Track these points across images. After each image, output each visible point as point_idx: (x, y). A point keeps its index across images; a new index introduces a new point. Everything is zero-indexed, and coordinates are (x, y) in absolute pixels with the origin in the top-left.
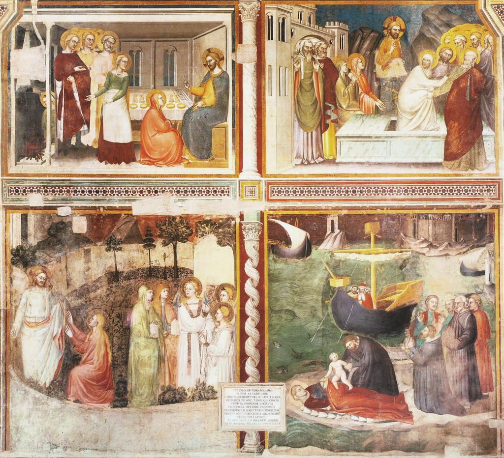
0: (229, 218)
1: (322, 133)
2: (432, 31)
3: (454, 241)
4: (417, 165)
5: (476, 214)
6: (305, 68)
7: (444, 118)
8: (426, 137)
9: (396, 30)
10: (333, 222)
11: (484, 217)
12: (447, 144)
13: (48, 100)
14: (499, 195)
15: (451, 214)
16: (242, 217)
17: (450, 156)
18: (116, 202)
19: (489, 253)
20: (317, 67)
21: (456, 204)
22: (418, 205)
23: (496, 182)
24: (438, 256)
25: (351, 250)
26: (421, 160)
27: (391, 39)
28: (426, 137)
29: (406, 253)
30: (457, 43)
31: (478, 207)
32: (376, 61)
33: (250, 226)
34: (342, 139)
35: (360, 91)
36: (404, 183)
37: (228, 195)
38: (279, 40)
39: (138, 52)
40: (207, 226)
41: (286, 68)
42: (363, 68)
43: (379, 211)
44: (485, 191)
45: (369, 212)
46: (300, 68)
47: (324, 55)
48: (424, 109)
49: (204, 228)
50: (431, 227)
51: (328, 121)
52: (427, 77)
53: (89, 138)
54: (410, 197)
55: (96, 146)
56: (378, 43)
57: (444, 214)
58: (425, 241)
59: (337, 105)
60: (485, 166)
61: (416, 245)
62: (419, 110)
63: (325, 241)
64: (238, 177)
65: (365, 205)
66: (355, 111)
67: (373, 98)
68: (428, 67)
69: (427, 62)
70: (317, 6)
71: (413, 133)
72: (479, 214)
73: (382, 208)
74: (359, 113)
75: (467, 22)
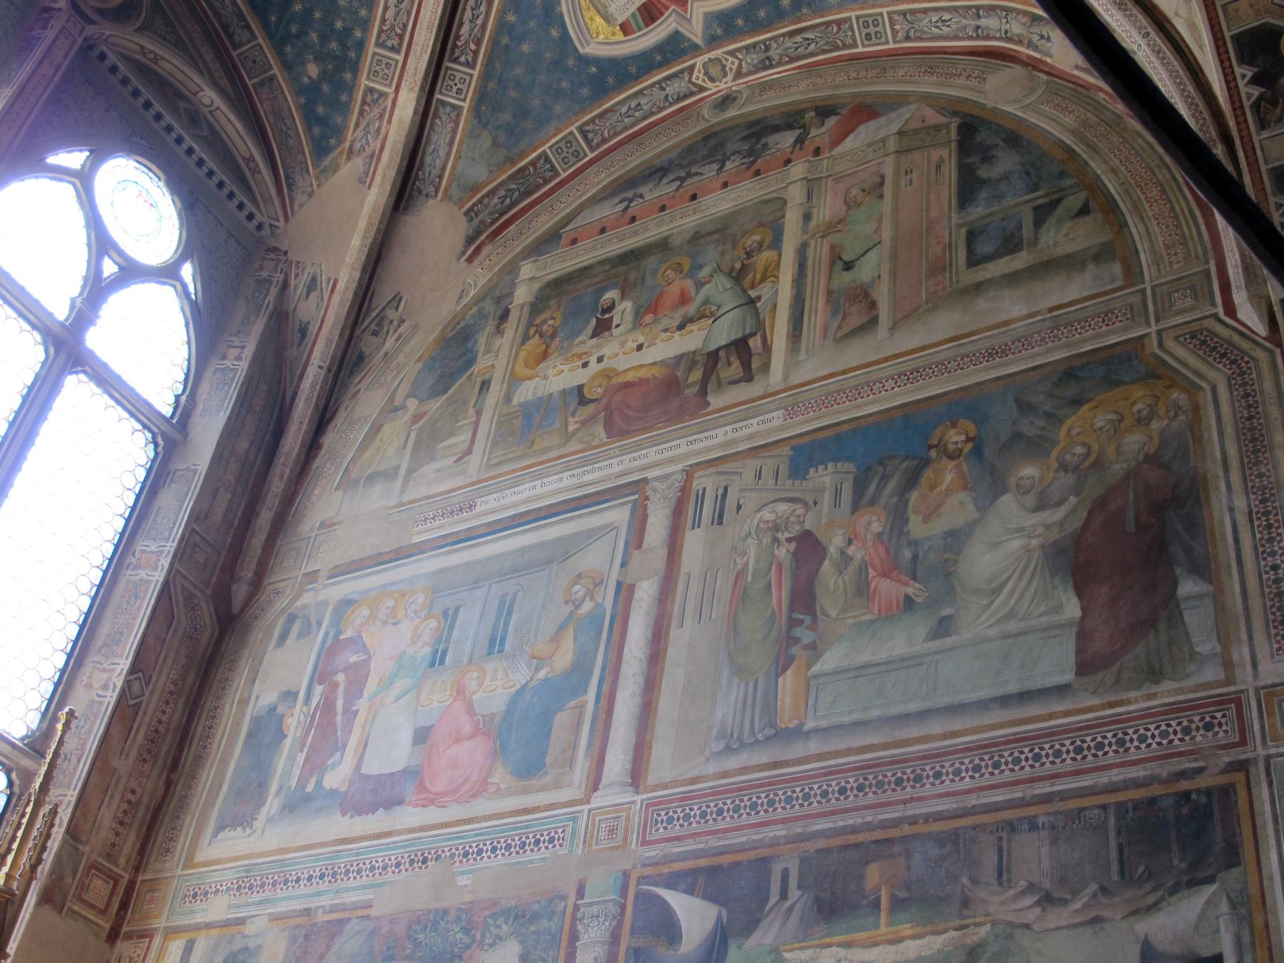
0: (554, 898)
1: (778, 675)
2: (1040, 423)
3: (1115, 877)
4: (1004, 701)
5: (1175, 794)
6: (757, 560)
7: (1071, 583)
8: (1025, 633)
9: (957, 443)
10: (785, 875)
11: (1204, 800)
12: (1083, 636)
13: (295, 722)
14: (1242, 732)
15: (1104, 807)
16: (580, 894)
17: (1085, 667)
18: (353, 893)
19: (1229, 898)
20: (783, 553)
21: (1115, 779)
22: (1008, 797)
23: (1230, 701)
24: (1068, 927)
25: (828, 940)
26: (1013, 688)
27: (945, 461)
28: (1025, 633)
29: (977, 930)
30: (1100, 428)
31: (1183, 774)
32: (910, 513)
33: (595, 909)
34: (821, 680)
35: (871, 572)
36: (969, 749)
37: (561, 845)
38: (712, 524)
39: (457, 610)
40: (506, 923)
41: (718, 569)
42: (880, 530)
43: (907, 829)
44: (1198, 729)
45: (879, 835)
46: (747, 562)
47: (797, 528)
48: (1019, 579)
49: (499, 927)
50: (1045, 851)
51: (795, 650)
52: (1026, 510)
53: (337, 777)
54: (987, 780)
55: (343, 789)
56: (919, 474)
57: (1081, 810)
58: (1031, 888)
59: (818, 613)
60: (1192, 668)
61: (1003, 903)
62: (1009, 579)
63: (763, 924)
64: (588, 802)
65: (869, 819)
66: (855, 617)
67: (900, 581)
68: (1029, 491)
69: (1028, 482)
70: (792, 448)
71: (993, 632)
72: (1186, 795)
73: (913, 821)
74: (868, 617)
75: (1120, 383)
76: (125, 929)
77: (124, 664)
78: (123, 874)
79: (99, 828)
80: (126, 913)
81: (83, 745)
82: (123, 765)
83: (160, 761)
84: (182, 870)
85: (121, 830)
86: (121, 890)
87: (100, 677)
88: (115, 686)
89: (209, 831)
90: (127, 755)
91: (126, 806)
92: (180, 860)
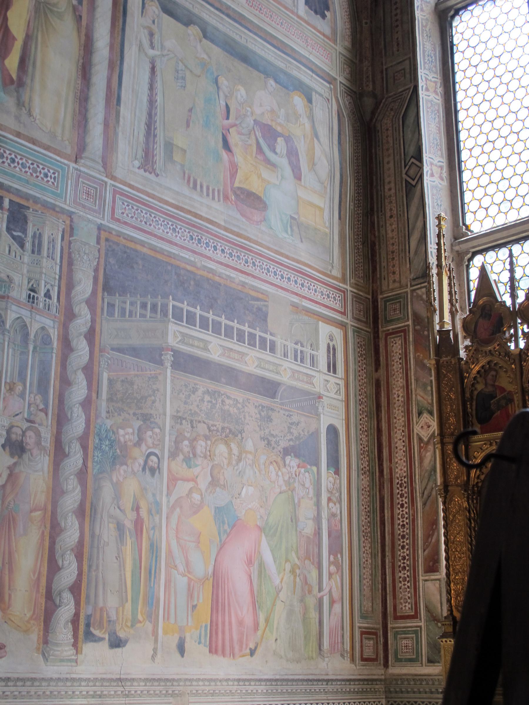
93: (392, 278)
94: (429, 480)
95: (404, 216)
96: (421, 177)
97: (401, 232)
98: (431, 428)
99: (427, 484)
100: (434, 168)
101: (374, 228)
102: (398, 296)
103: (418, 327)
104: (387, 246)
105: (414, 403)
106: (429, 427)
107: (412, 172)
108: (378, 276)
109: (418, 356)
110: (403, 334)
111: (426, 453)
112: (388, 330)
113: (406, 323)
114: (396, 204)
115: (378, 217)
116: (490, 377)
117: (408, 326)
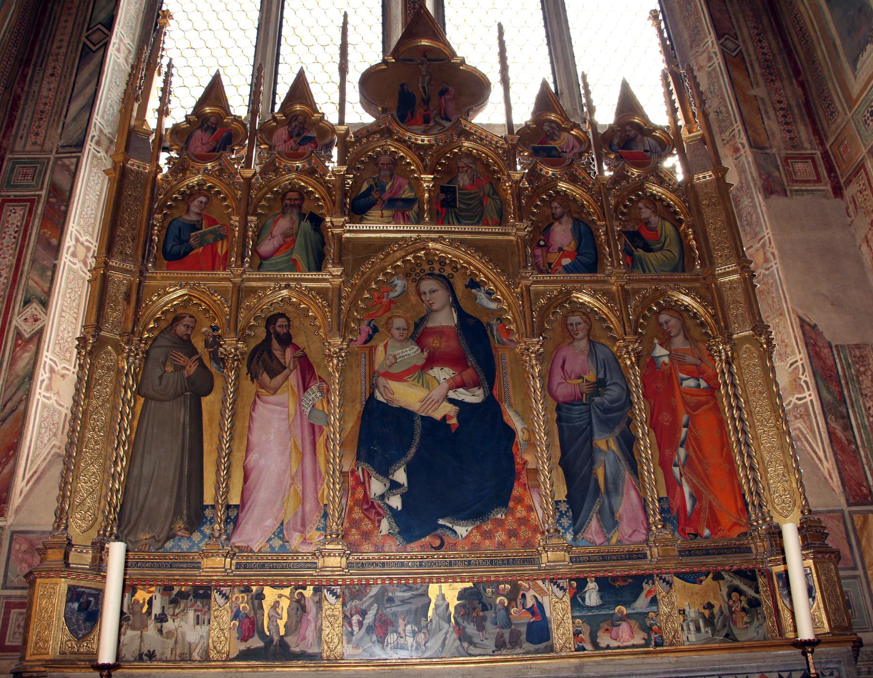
76: (842, 181)
77: (711, 39)
78: (814, 152)
79: (773, 134)
80: (835, 172)
81: (723, 99)
82: (760, 91)
83: (784, 76)
84: (850, 109)
85: (790, 128)
86: (820, 163)
87: (703, 60)
88: (715, 53)
89: (847, 66)
90: (757, 84)
91: (782, 113)
92: (843, 108)
93: (33, 138)
94: (18, 389)
95: (70, 78)
96: (106, 46)
97: (61, 93)
98: (38, 323)
99: (14, 394)
100: (122, 45)
101: (24, 80)
102: (36, 161)
103: (53, 200)
104: (36, 103)
105: (21, 288)
106: (36, 320)
107: (95, 37)
108: (13, 133)
109: (44, 232)
110: (29, 204)
111: (24, 353)
112: (9, 196)
113: (37, 193)
114: (64, 64)
115: (34, 72)
116: (196, 202)
117: (40, 196)
